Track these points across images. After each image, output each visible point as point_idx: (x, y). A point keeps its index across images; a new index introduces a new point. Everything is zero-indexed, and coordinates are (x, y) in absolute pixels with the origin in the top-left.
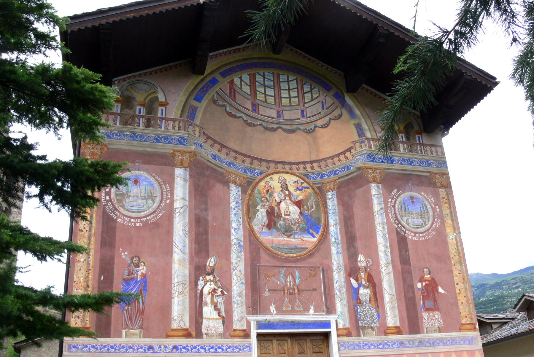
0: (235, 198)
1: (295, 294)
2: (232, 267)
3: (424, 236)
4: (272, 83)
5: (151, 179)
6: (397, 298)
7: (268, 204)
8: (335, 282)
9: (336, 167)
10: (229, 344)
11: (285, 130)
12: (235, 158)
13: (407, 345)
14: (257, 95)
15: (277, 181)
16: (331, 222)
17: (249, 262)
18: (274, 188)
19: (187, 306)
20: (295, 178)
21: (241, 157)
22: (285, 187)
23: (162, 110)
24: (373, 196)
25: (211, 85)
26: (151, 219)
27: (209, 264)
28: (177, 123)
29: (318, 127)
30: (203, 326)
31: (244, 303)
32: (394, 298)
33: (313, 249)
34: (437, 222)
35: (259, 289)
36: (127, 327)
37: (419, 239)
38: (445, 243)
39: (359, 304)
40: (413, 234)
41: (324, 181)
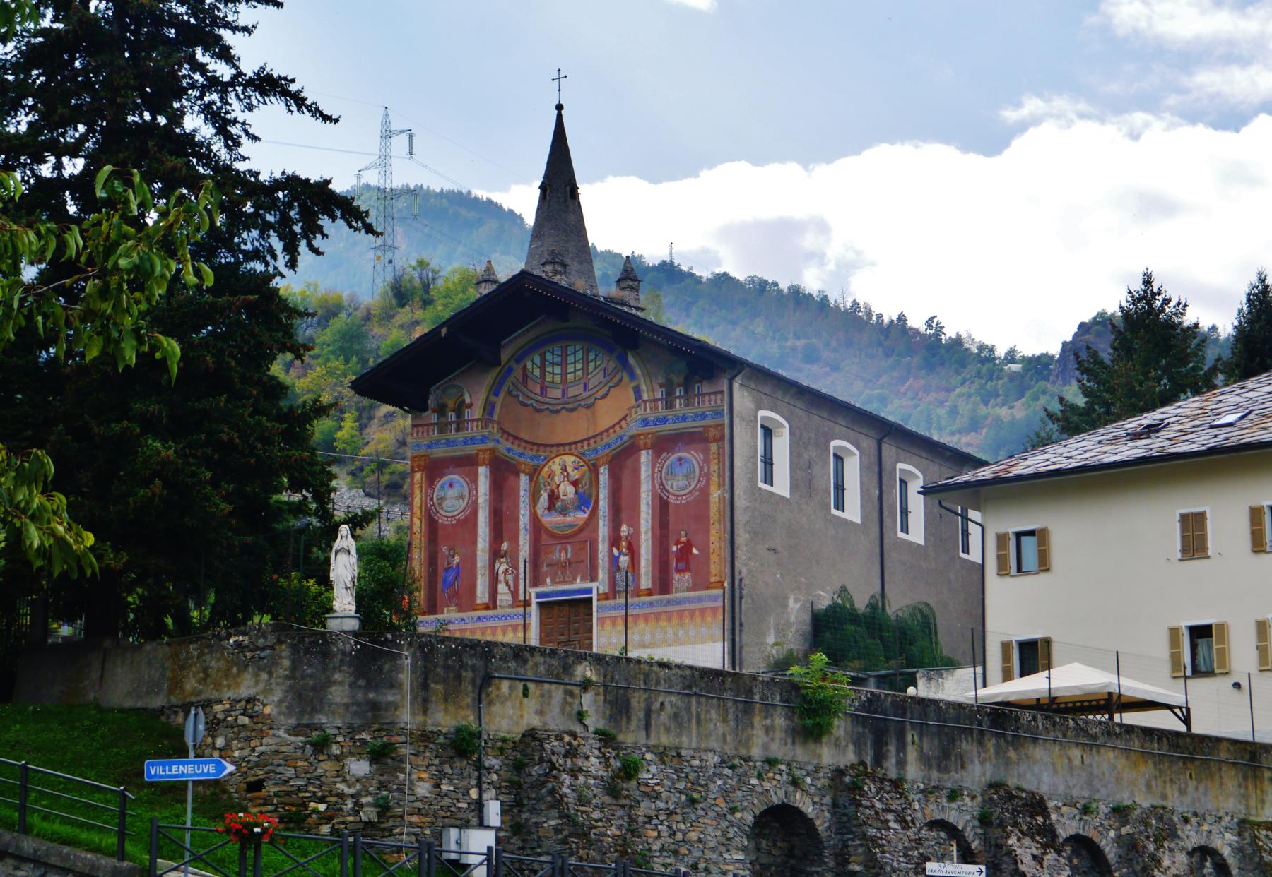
5: (461, 480)
16: (601, 496)
20: (573, 458)
21: (529, 446)
22: (564, 469)
26: (462, 516)
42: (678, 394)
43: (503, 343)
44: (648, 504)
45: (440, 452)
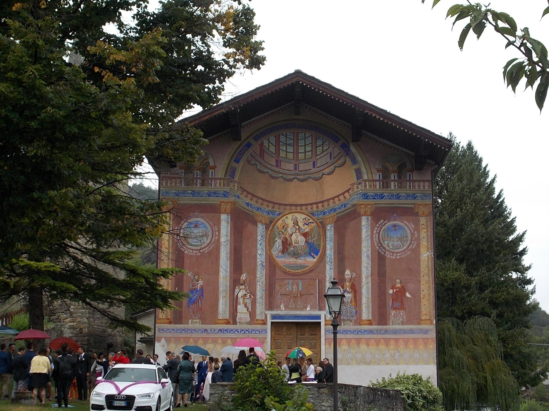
3: (401, 255)
4: (292, 141)
5: (206, 223)
6: (372, 300)
9: (336, 206)
11: (299, 180)
13: (375, 332)
19: (228, 305)
20: (304, 216)
21: (266, 203)
22: (296, 223)
23: (212, 172)
26: (206, 250)
28: (222, 181)
31: (264, 303)
34: (413, 244)
36: (192, 318)
37: (396, 257)
38: (417, 259)
40: (392, 254)
41: (325, 217)
42: (392, 178)
43: (243, 124)
44: (368, 256)
45: (186, 200)
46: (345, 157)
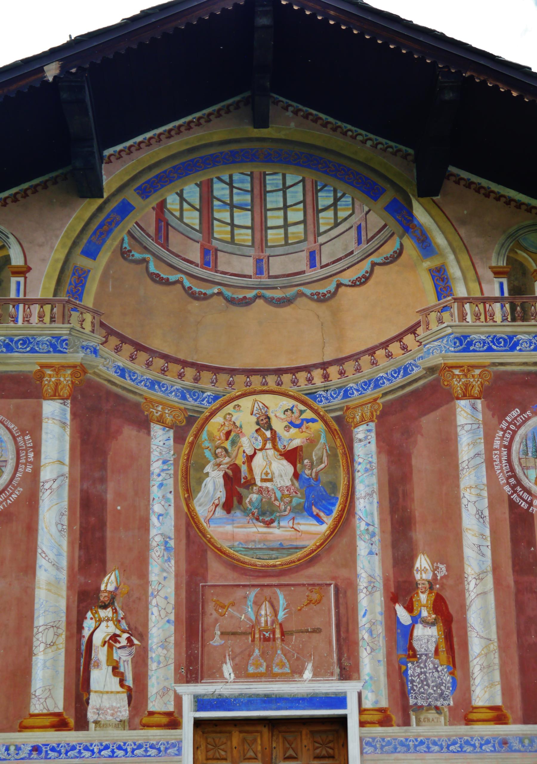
0: (161, 453)
1: (274, 639)
2: (150, 590)
4: (248, 197)
6: (499, 647)
7: (227, 460)
8: (361, 613)
10: (138, 740)
11: (270, 301)
12: (164, 371)
14: (216, 229)
15: (249, 411)
16: (361, 489)
17: (184, 580)
18: (241, 427)
20: (288, 403)
21: (175, 368)
24: (459, 429)
25: (118, 218)
27: (106, 586)
29: (346, 286)
30: (90, 708)
31: (172, 661)
32: (492, 646)
33: (318, 547)
35: (203, 631)
39: (412, 659)
41: (349, 404)
44: (480, 515)
46: (401, 237)
